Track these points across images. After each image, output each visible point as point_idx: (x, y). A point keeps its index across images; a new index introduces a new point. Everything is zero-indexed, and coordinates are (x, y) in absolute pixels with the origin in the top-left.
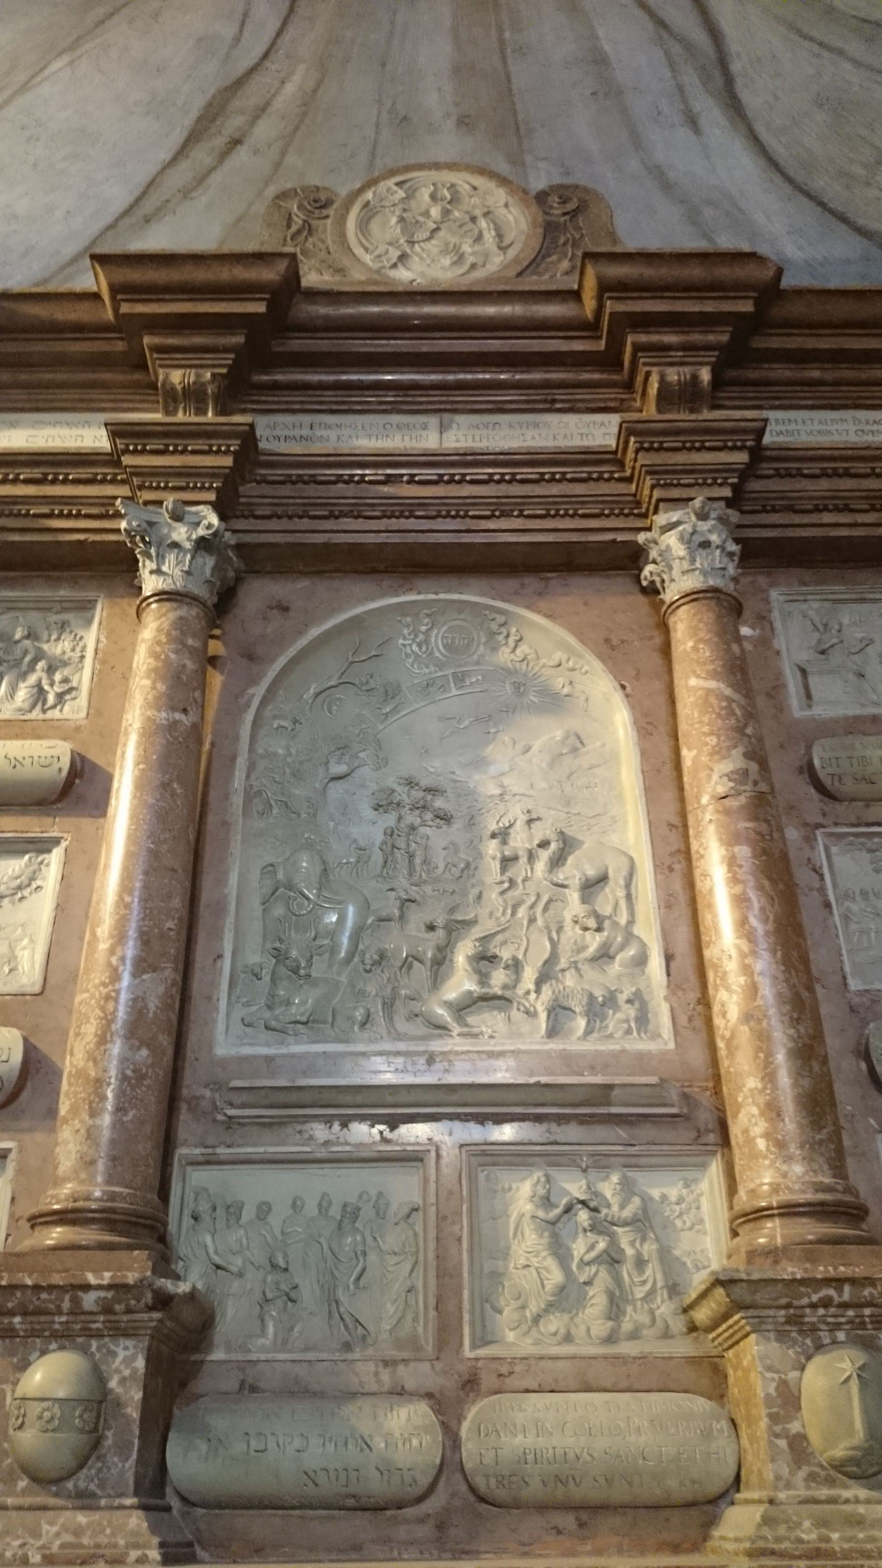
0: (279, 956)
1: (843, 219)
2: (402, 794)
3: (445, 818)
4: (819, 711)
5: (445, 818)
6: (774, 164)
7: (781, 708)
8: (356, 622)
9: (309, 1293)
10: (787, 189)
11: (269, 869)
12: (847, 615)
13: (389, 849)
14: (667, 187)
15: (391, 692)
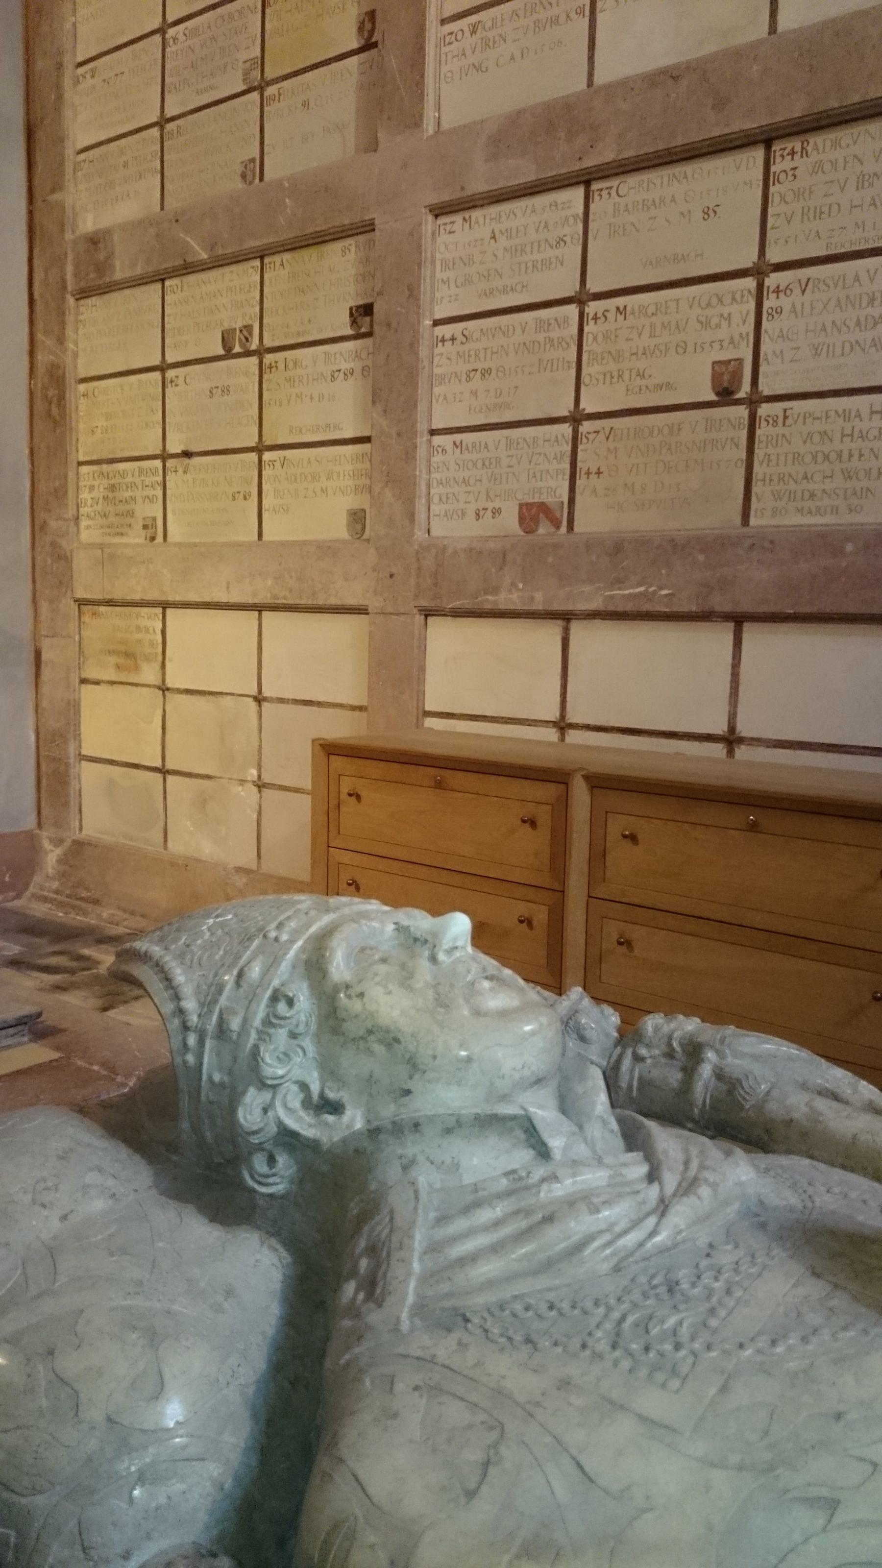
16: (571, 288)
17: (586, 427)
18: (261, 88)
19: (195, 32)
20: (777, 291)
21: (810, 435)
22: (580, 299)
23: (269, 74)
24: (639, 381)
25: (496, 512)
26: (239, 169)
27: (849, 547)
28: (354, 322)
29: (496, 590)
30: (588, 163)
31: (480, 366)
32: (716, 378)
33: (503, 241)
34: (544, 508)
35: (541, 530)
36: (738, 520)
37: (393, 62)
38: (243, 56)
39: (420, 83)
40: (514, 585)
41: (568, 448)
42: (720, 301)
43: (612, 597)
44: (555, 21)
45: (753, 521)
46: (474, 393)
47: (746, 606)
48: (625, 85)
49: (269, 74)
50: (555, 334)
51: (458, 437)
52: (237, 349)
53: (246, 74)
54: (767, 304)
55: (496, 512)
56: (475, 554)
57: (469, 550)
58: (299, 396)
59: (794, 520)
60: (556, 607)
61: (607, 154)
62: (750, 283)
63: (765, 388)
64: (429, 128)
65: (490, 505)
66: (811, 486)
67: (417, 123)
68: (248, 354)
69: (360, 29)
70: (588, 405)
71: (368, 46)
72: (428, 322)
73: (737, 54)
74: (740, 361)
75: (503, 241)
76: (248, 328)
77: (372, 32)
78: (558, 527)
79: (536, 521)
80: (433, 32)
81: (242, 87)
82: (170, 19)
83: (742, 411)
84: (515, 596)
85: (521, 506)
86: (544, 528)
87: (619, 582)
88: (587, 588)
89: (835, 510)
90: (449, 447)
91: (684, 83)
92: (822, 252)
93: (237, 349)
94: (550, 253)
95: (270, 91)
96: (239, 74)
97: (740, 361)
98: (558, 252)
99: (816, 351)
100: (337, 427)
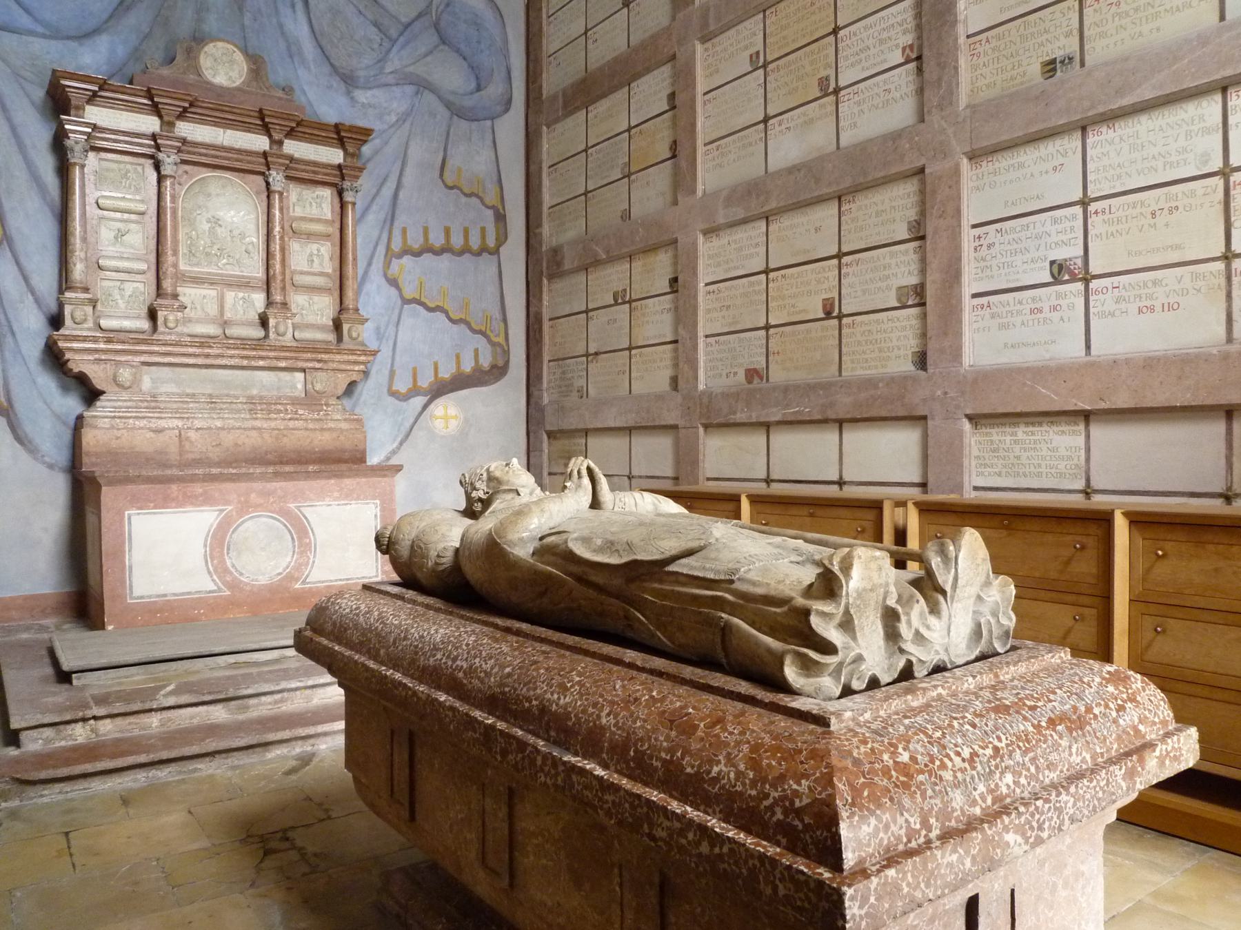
0: (190, 252)
1: (328, 59)
2: (212, 220)
3: (220, 226)
4: (296, 214)
5: (220, 226)
6: (313, 31)
7: (289, 212)
8: (203, 178)
9: (198, 307)
10: (315, 44)
11: (187, 234)
12: (304, 192)
13: (209, 231)
14: (283, 33)
15: (209, 195)
16: (762, 267)
17: (772, 331)
18: (629, 176)
19: (600, 151)
20: (847, 265)
21: (864, 332)
22: (767, 271)
23: (633, 170)
24: (792, 309)
25: (735, 374)
26: (620, 214)
27: (881, 385)
28: (671, 286)
29: (735, 413)
30: (766, 208)
31: (726, 304)
32: (824, 306)
33: (733, 246)
34: (755, 371)
35: (755, 382)
36: (837, 374)
37: (683, 164)
38: (621, 162)
39: (695, 174)
40: (743, 410)
41: (764, 341)
42: (824, 270)
43: (785, 414)
44: (750, 144)
45: (843, 374)
46: (724, 317)
47: (841, 416)
48: (779, 173)
49: (633, 170)
50: (757, 288)
51: (717, 338)
52: (620, 301)
53: (622, 169)
54: (843, 272)
55: (735, 374)
56: (725, 396)
57: (723, 393)
58: (648, 322)
59: (859, 372)
60: (762, 420)
61: (773, 204)
62: (835, 261)
63: (845, 311)
64: (699, 193)
65: (733, 371)
66: (866, 356)
67: (694, 192)
68: (624, 303)
69: (671, 149)
70: (772, 322)
71: (674, 156)
72: (702, 285)
73: (822, 159)
74: (833, 298)
75: (733, 246)
76: (625, 290)
77: (675, 150)
78: (762, 379)
79: (752, 377)
80: (701, 150)
81: (620, 176)
82: (589, 145)
83: (835, 322)
84: (743, 415)
85: (746, 370)
86: (756, 380)
87: (787, 406)
88: (774, 410)
89: (876, 367)
90: (714, 343)
91: (802, 172)
92: (864, 246)
93: (620, 301)
94: (753, 250)
95: (633, 177)
96: (619, 170)
97: (833, 298)
98: (757, 250)
99: (864, 292)
100: (664, 336)
